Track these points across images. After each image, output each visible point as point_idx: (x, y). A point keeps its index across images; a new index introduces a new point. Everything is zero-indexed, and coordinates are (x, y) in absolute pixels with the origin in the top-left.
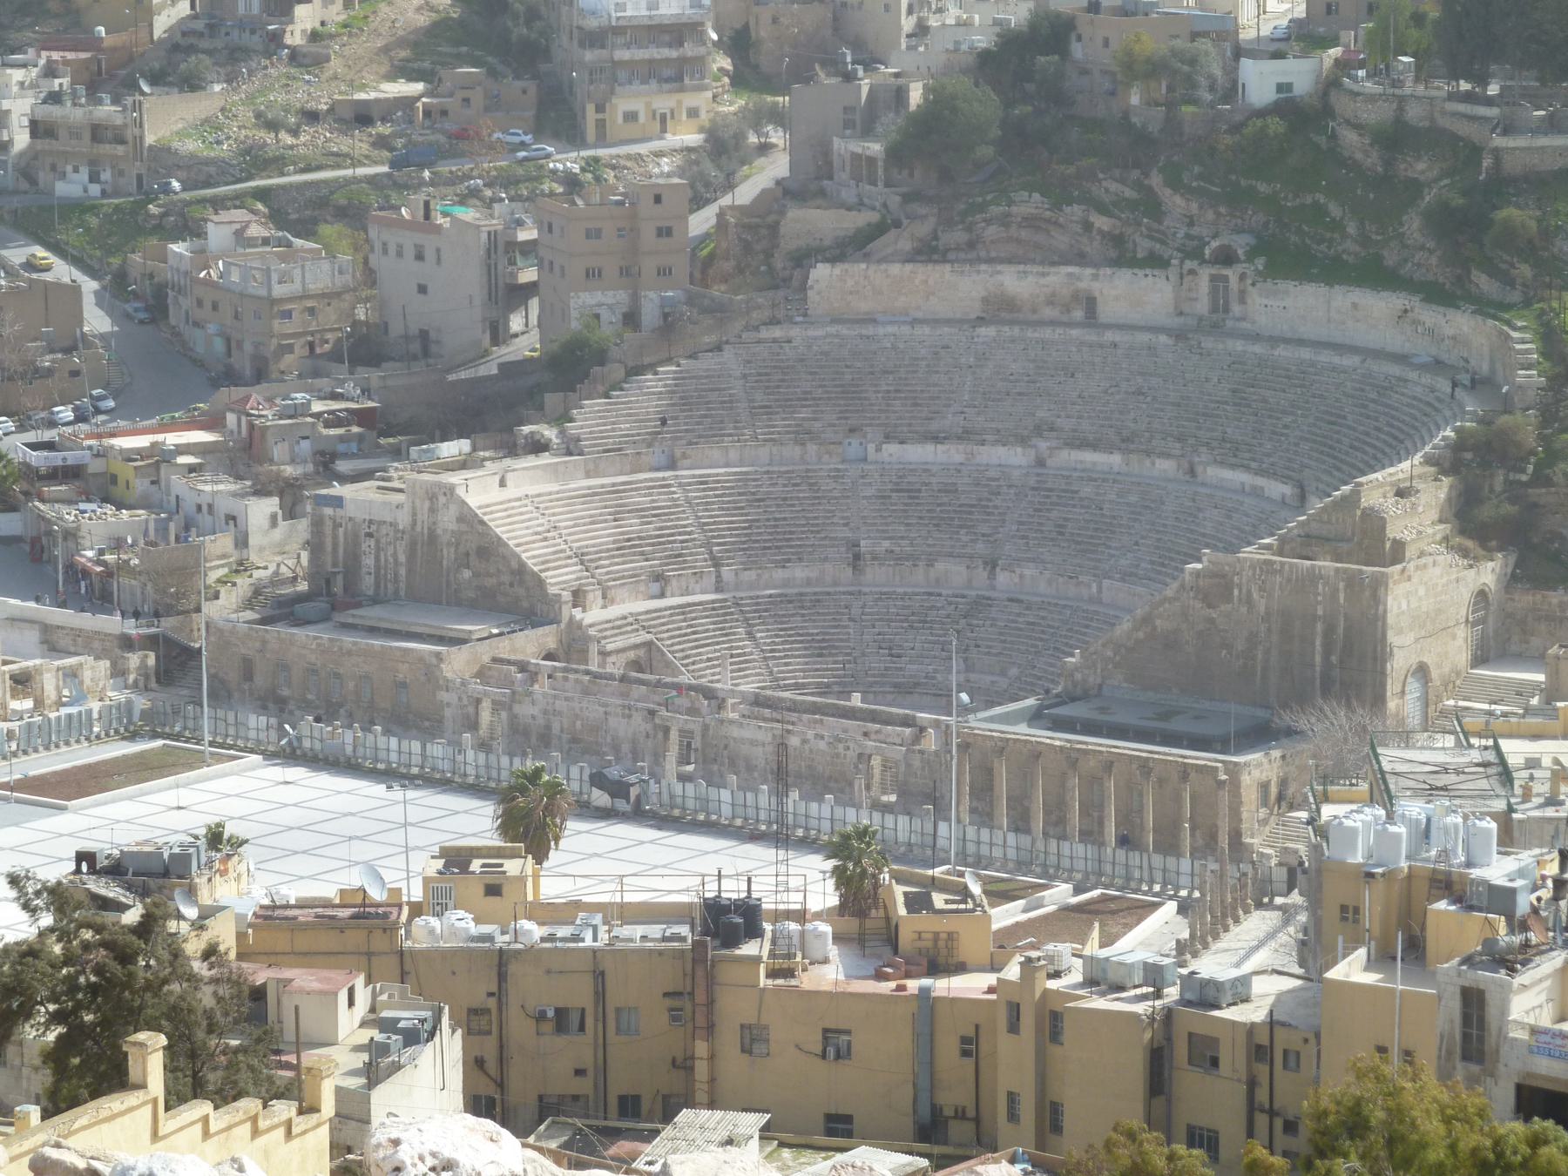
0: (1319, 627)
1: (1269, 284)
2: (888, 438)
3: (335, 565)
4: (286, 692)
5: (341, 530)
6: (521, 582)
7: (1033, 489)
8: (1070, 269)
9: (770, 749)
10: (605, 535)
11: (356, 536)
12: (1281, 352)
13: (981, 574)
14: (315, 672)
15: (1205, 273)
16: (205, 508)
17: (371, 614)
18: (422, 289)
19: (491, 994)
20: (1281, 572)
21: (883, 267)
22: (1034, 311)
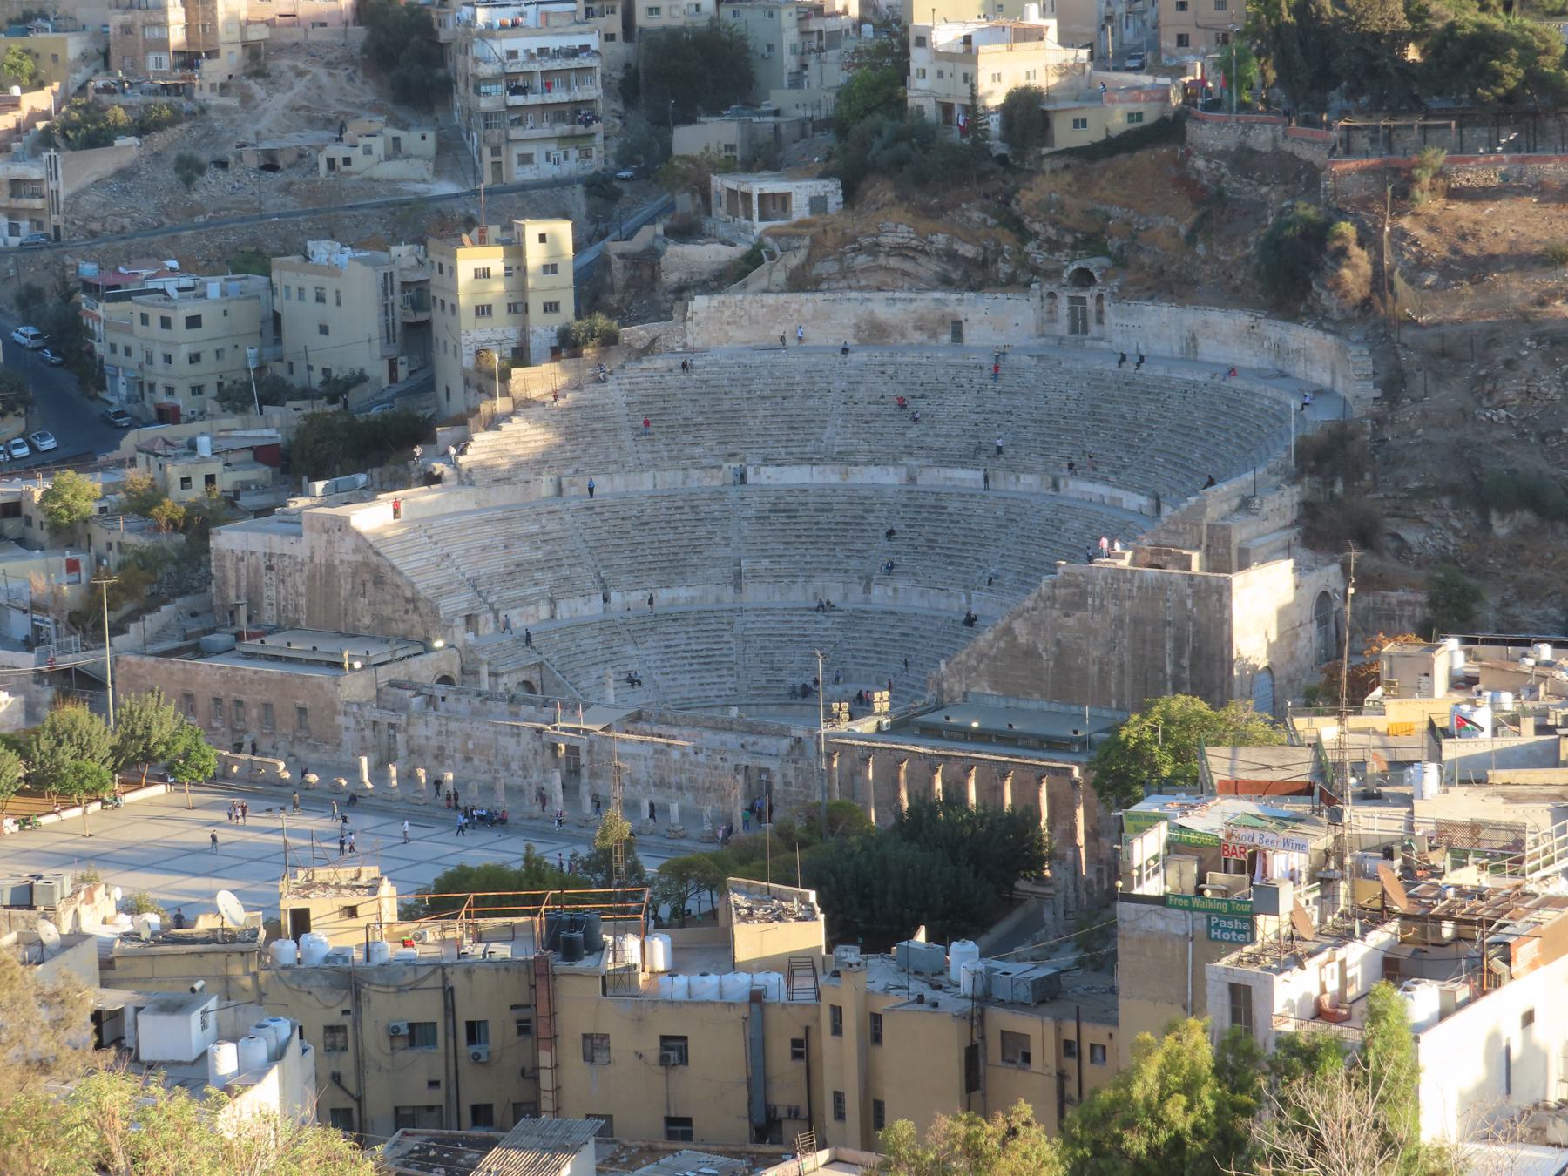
0: (1169, 631)
2: (767, 461)
3: (238, 597)
5: (242, 565)
6: (416, 608)
7: (905, 506)
8: (937, 295)
9: (651, 763)
10: (495, 564)
11: (257, 569)
13: (857, 591)
14: (218, 700)
16: (115, 546)
17: (273, 643)
19: (345, 1012)
20: (1130, 581)
21: (759, 297)
22: (903, 335)
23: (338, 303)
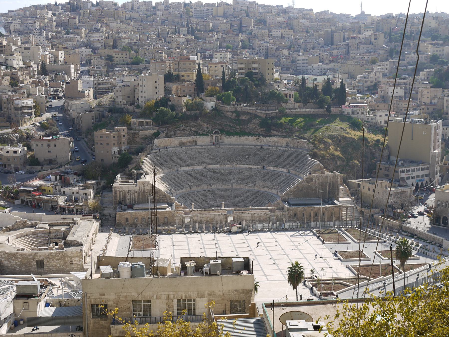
1: (228, 136)
3: (120, 199)
4: (137, 223)
5: (121, 193)
6: (165, 197)
11: (125, 193)
12: (236, 146)
15: (214, 136)
18: (50, 152)
23: (55, 146)
